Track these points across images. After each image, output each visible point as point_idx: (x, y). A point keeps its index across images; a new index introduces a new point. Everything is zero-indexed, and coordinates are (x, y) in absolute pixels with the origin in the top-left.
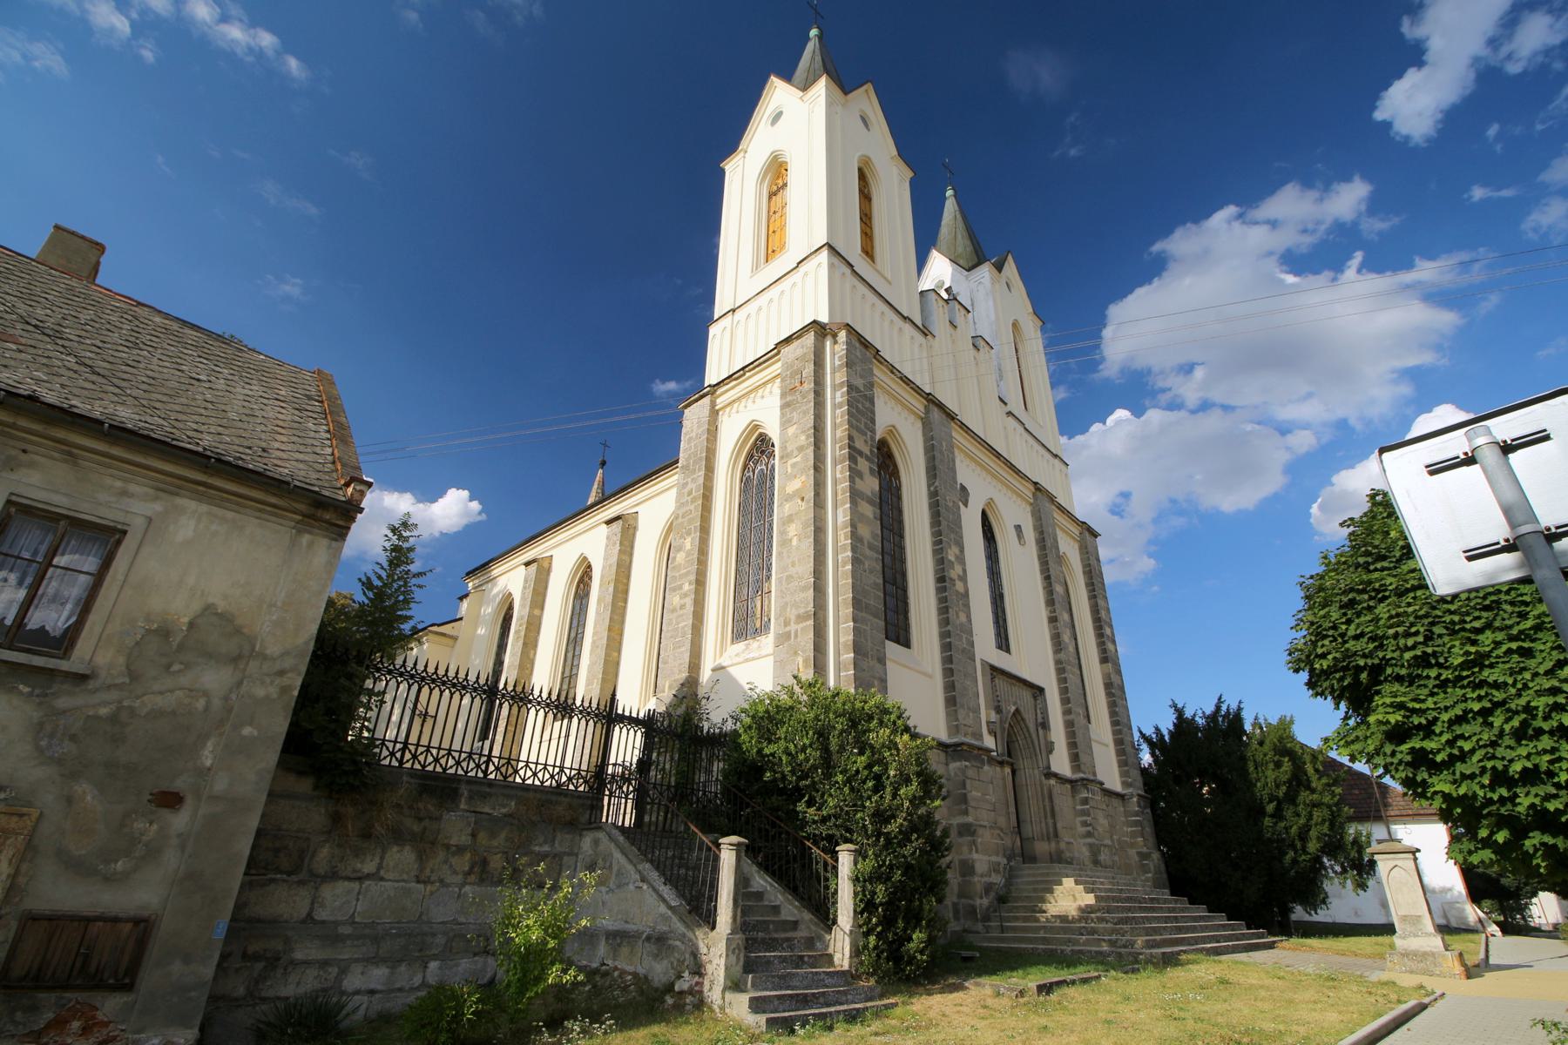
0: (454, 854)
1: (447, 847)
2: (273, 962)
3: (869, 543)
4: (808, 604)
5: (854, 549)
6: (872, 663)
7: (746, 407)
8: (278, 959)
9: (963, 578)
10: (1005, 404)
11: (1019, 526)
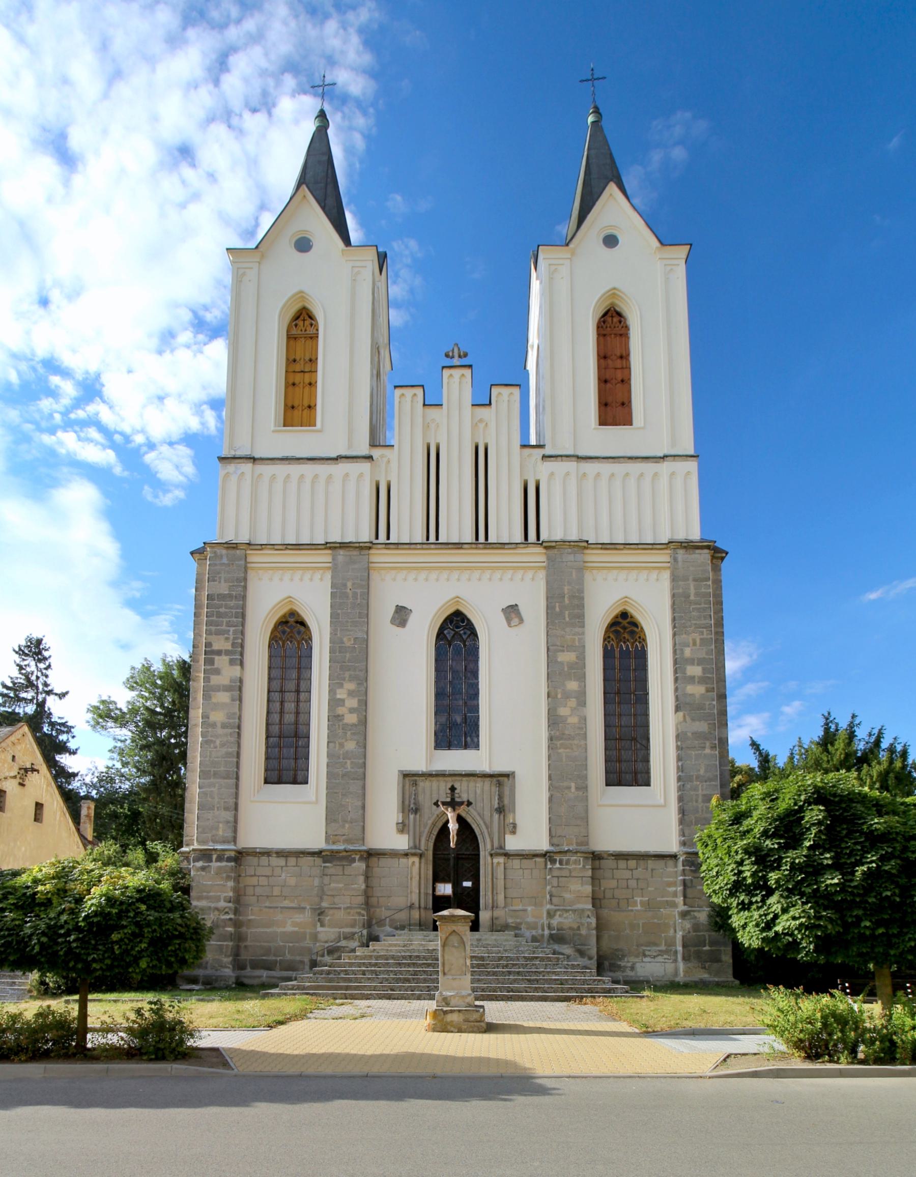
6: (217, 812)
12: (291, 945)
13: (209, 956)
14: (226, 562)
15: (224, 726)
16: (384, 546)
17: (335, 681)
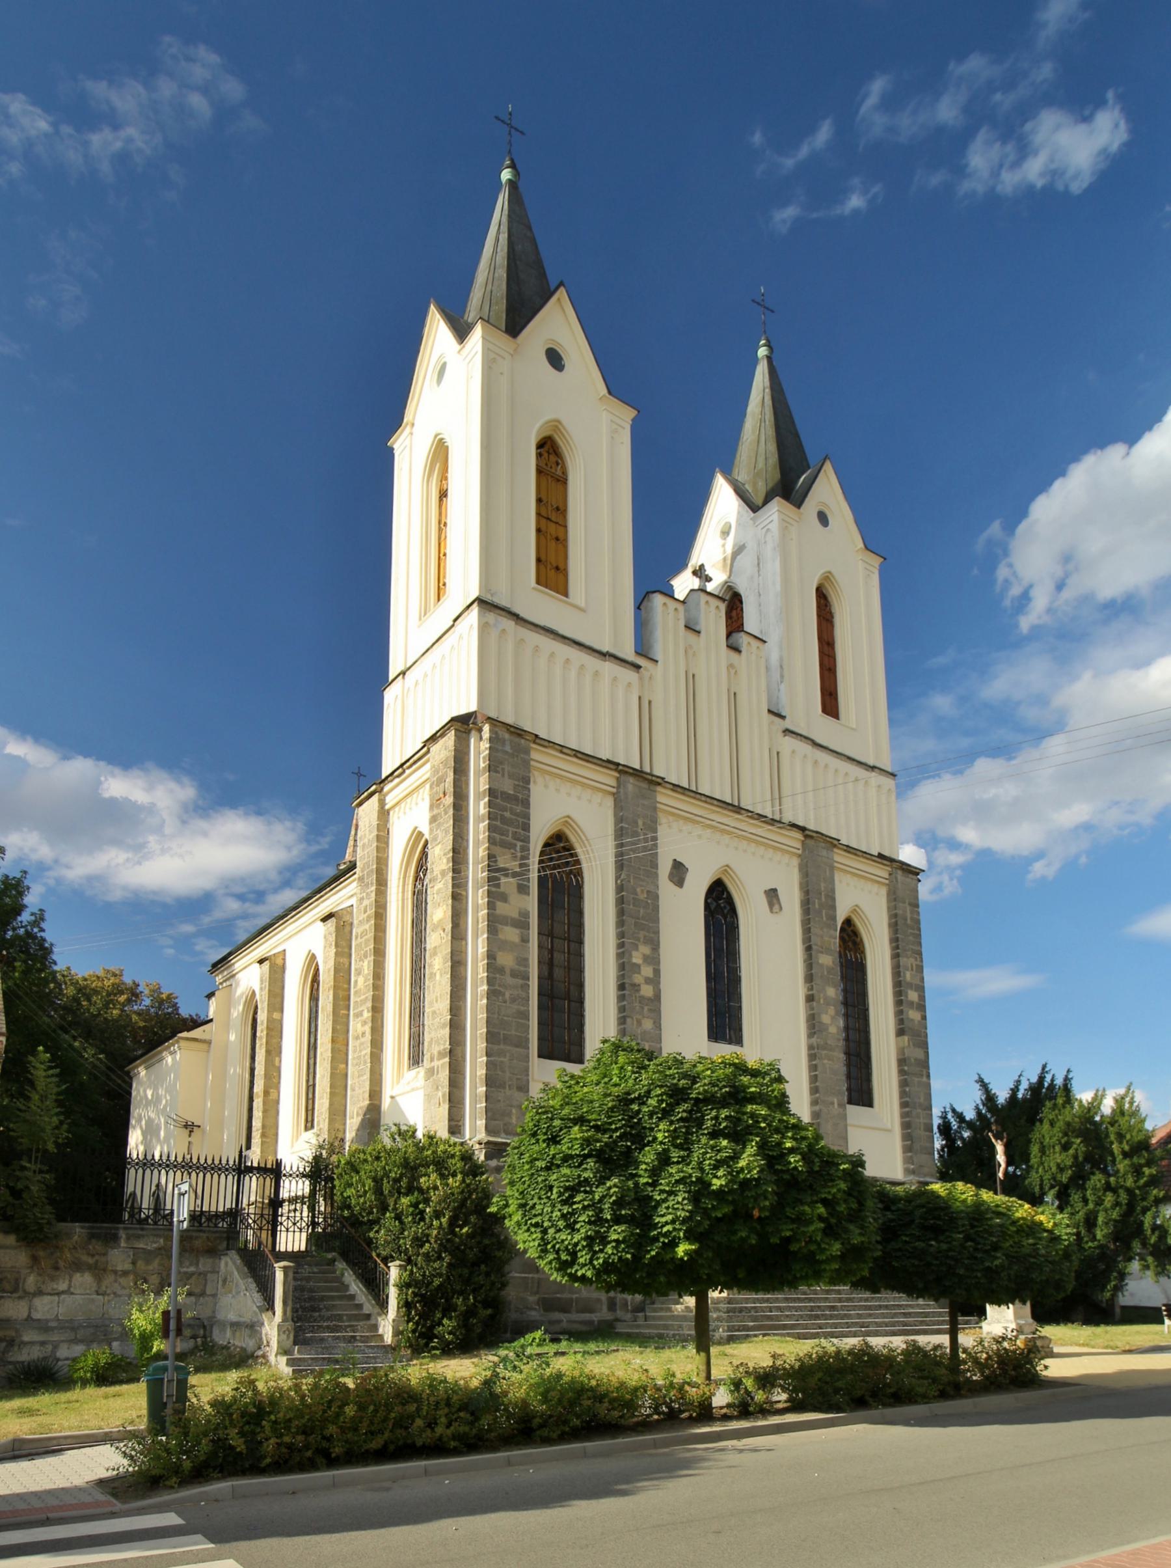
0: (121, 1276)
1: (115, 1272)
2: (11, 1343)
3: (512, 970)
4: (445, 1041)
5: (490, 981)
6: (508, 1092)
7: (417, 804)
8: (13, 1341)
9: (655, 980)
10: (783, 717)
11: (774, 891)
13: (512, 1293)
14: (510, 751)
16: (671, 786)
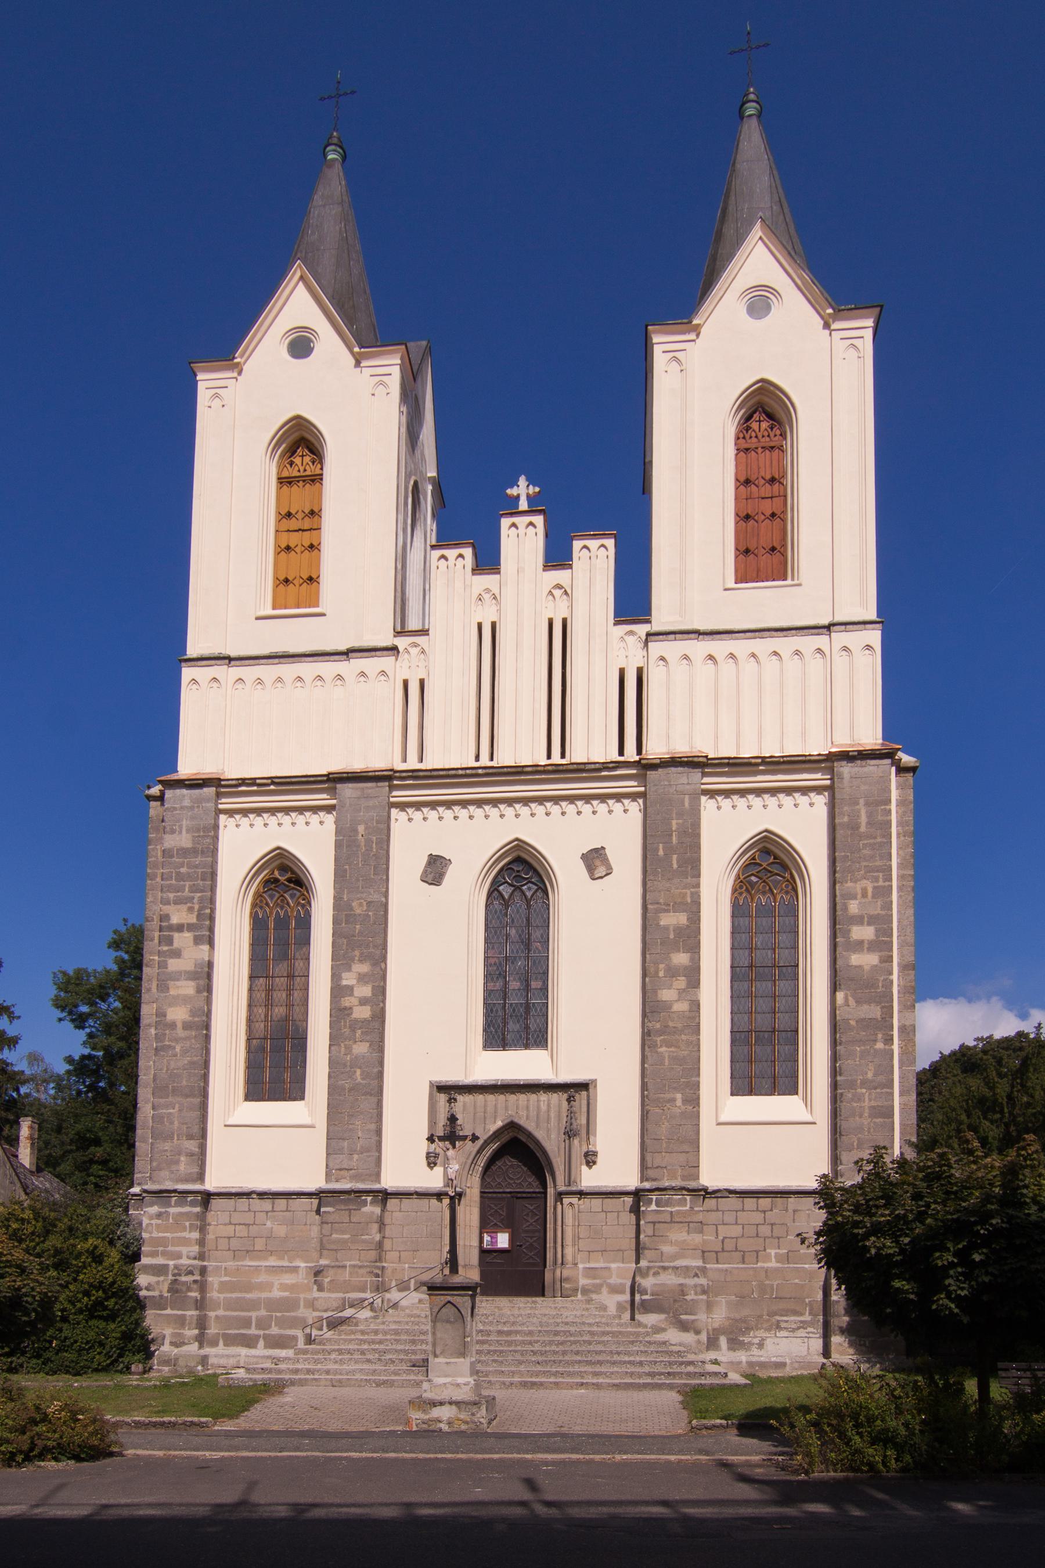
12: (278, 1314)
15: (187, 1026)
17: (340, 961)
